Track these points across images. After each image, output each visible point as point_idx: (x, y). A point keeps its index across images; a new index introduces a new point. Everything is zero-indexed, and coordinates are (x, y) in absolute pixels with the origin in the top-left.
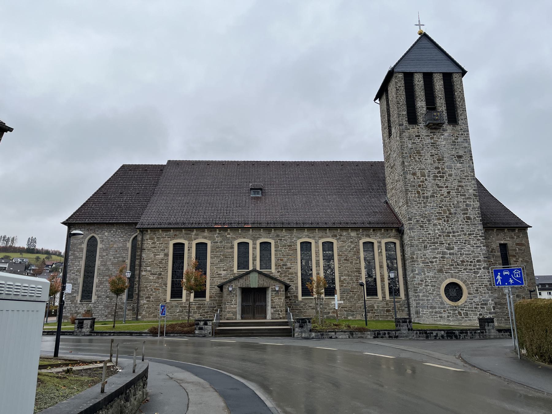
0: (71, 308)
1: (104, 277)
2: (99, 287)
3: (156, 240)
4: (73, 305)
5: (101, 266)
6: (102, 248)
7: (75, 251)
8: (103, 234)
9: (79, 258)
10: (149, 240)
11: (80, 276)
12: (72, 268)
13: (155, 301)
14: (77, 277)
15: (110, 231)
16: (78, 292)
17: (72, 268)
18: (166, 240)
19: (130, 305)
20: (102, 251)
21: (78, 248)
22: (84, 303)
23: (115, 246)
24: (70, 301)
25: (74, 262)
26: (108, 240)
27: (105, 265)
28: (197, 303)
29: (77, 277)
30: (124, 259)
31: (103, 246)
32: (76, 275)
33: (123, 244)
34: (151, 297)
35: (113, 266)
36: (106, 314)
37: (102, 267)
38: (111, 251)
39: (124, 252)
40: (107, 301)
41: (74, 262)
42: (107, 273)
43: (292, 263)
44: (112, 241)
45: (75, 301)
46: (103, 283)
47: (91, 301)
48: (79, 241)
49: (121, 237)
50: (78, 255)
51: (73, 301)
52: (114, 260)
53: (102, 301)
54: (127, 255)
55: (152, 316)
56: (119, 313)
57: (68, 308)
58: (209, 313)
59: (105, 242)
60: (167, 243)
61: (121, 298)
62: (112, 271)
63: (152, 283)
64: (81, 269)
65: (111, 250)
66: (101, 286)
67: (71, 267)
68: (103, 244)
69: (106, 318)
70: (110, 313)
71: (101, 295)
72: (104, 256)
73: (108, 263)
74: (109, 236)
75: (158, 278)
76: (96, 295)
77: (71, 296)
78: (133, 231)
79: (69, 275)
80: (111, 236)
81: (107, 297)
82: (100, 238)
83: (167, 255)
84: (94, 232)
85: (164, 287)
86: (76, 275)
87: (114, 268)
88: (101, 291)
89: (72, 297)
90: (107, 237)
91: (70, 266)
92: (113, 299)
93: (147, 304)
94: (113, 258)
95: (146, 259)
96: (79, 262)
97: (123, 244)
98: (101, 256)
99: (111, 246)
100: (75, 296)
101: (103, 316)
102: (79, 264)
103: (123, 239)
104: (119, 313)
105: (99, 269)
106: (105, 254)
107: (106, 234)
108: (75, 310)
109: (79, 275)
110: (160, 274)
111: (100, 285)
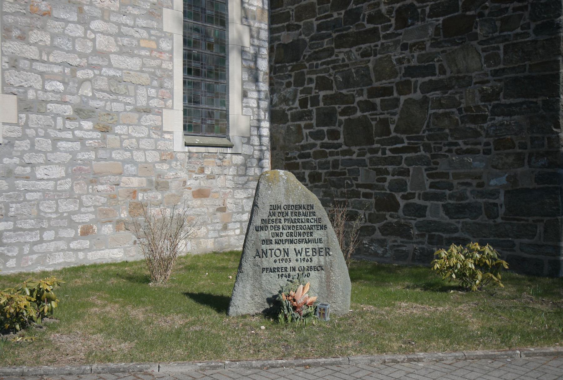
2: (22, 38)
19: (202, 170)
36: (86, 218)
40: (81, 140)
61: (159, 129)
66: (35, 36)
69: (86, 243)
70: (106, 214)
88: (41, 67)
101: (71, 233)
111: (31, 27)
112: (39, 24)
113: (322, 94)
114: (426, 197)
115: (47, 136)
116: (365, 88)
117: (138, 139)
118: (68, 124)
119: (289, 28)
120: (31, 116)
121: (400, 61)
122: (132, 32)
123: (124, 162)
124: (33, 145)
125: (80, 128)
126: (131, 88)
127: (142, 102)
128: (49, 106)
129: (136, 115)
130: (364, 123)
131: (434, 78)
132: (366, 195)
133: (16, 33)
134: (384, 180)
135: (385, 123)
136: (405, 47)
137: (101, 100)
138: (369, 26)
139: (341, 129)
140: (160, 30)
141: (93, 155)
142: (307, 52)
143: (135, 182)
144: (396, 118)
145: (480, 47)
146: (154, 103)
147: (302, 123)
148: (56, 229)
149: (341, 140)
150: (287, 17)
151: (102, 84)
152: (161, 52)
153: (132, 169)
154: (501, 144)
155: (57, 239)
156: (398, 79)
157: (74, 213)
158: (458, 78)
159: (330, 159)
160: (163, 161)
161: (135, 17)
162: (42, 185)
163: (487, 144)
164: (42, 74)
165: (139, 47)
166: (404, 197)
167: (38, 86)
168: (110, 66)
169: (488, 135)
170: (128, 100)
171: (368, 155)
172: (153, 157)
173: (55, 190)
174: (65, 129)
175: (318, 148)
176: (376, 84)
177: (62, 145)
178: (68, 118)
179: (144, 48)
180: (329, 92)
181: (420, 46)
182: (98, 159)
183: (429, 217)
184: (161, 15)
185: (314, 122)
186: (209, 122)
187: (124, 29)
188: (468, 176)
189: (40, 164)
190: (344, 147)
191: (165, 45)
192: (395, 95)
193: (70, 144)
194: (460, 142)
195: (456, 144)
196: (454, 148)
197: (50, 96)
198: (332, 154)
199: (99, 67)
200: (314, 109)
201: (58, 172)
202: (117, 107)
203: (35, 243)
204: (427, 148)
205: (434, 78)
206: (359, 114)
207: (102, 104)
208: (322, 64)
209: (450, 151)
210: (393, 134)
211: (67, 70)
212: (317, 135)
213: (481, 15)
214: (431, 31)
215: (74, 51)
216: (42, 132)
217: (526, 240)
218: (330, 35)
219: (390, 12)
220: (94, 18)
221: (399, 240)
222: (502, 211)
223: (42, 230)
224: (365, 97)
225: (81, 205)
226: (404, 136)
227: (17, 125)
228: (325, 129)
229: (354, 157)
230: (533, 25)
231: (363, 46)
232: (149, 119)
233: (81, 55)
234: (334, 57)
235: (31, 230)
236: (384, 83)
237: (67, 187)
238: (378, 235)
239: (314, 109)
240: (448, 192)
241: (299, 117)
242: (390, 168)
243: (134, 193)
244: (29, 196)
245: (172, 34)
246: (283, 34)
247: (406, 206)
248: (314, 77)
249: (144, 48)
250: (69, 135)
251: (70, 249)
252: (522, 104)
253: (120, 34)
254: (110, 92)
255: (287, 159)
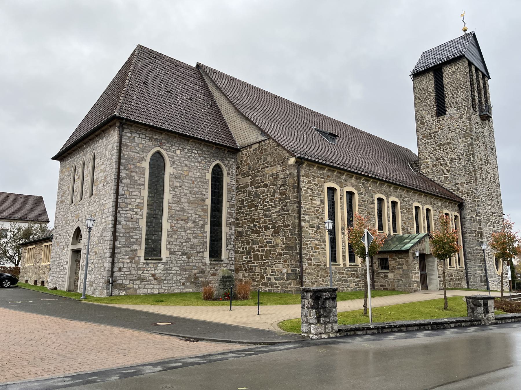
0: (130, 271)
1: (179, 222)
2: (171, 237)
3: (311, 178)
4: (134, 265)
5: (172, 203)
6: (173, 174)
7: (131, 171)
8: (174, 152)
9: (139, 185)
10: (304, 177)
11: (142, 215)
12: (128, 201)
13: (316, 265)
14: (138, 217)
15: (183, 149)
16: (141, 242)
17: (128, 201)
18: (321, 181)
19: (214, 268)
20: (173, 180)
21: (136, 167)
22: (151, 263)
23: (191, 174)
24: (129, 258)
25: (131, 190)
26: (181, 163)
27: (178, 202)
28: (352, 269)
29: (138, 217)
30: (204, 197)
31: (175, 171)
32: (136, 213)
33: (201, 173)
34: (312, 259)
35: (189, 206)
36: (183, 281)
37: (174, 205)
38: (186, 181)
39: (203, 186)
40: (183, 261)
41: (131, 190)
42: (181, 215)
43: (411, 228)
44: (186, 166)
45: (137, 258)
46: (177, 230)
47: (162, 260)
48: (138, 155)
49: (198, 162)
50: (137, 178)
51: (134, 258)
52: (190, 195)
53: (177, 259)
54: (207, 191)
55: (315, 285)
56: (200, 279)
57: (125, 270)
58: (361, 282)
59: (178, 165)
60: (322, 186)
61: (202, 257)
62: (188, 213)
63: (312, 239)
64: (143, 203)
65: (185, 179)
66: (174, 236)
67: (126, 198)
68: (174, 168)
69: (183, 287)
71: (175, 250)
72: (177, 187)
73: (183, 200)
74: (182, 157)
75: (316, 232)
76: (167, 249)
77: (128, 249)
78: (213, 157)
79: (124, 212)
80: (185, 158)
81: (184, 254)
82: (169, 157)
83: (322, 201)
84: (160, 145)
85: (323, 246)
86: (136, 213)
87: (190, 208)
88: (175, 243)
89: (132, 251)
90: (179, 157)
91: (125, 196)
92: (192, 258)
93: (309, 269)
94: (188, 192)
95: (304, 204)
96: (140, 192)
97: (201, 173)
98: (173, 188)
99: (185, 174)
100: (136, 250)
101: (179, 284)
102: (139, 194)
103: (201, 165)
104: (200, 279)
105: (170, 208)
106: (178, 185)
107: (178, 152)
108: (137, 274)
109: (141, 213)
110: (318, 228)
111: (173, 234)
112: (175, 233)
113: (248, 246)
114: (271, 275)
115: (175, 260)
116: (258, 246)
117: (197, 260)
118: (180, 257)
119: (240, 227)
120: (172, 255)
121: (265, 239)
122: (197, 232)
123: (193, 266)
124: (172, 262)
125: (183, 258)
126: (196, 246)
127: (198, 250)
128: (176, 253)
129: (197, 254)
130: (257, 255)
131: (272, 244)
132: (258, 275)
133: (170, 236)
134: (262, 271)
135: (262, 255)
136: (266, 236)
137: (188, 250)
138: (258, 229)
139: (252, 256)
140: (204, 231)
141: (185, 264)
142: (244, 234)
143: (196, 271)
144: (264, 254)
145: (280, 238)
146: (201, 250)
147: (243, 254)
148: (176, 283)
149: (252, 260)
150: (239, 224)
151: (189, 246)
152: (203, 236)
153: (195, 268)
154: (285, 262)
155: (176, 286)
156: (264, 244)
157: (180, 279)
158: (276, 245)
159: (250, 265)
160: (204, 266)
161: (197, 228)
162: (173, 272)
163: (282, 262)
164: (175, 245)
165: (198, 236)
166: (266, 275)
167: (174, 248)
168: (191, 241)
169: (282, 260)
170: (195, 250)
171: (258, 264)
172: (200, 264)
173: (176, 273)
174: (179, 258)
175: (247, 262)
176: (260, 245)
177: (178, 262)
178: (180, 255)
179: (199, 236)
180: (249, 246)
181: (269, 236)
182: (187, 266)
183: (271, 281)
184: (204, 227)
185: (246, 254)
186: (217, 254)
187: (195, 232)
188: (279, 270)
189: (173, 267)
190: (253, 262)
191: (205, 235)
192: (264, 248)
193: (180, 262)
194: (277, 261)
195: (276, 261)
196: (276, 262)
197: (176, 250)
198: (250, 263)
199: (188, 242)
200: (246, 250)
201: (177, 269)
202: (192, 252)
203: (171, 287)
204: (271, 262)
205: (272, 244)
206: (256, 252)
207: (188, 251)
208: (248, 238)
209: (275, 263)
210: (264, 258)
211: (181, 243)
212: (246, 258)
213: (281, 230)
214: (271, 232)
215: (182, 239)
216: (174, 259)
217: (290, 286)
218: (250, 230)
219: (263, 226)
220: (187, 230)
221: (265, 287)
222: (285, 279)
223: (173, 283)
224: (257, 248)
225: (182, 277)
226: (266, 259)
227: (169, 257)
228: (248, 256)
229: (255, 264)
230: (290, 234)
231: (257, 234)
232: (200, 255)
233: (184, 240)
234: (250, 237)
235: (171, 283)
236: (262, 245)
237: (179, 272)
238: (260, 286)
239: (246, 250)
240: (275, 274)
241: (242, 252)
242: (263, 267)
243: (195, 274)
244: (170, 275)
245: (207, 232)
246: (239, 228)
247: (267, 278)
248: (246, 241)
249: (199, 236)
250: (180, 260)
251: (179, 289)
252: (288, 252)
253: (194, 233)
254: (190, 248)
255: (239, 265)
